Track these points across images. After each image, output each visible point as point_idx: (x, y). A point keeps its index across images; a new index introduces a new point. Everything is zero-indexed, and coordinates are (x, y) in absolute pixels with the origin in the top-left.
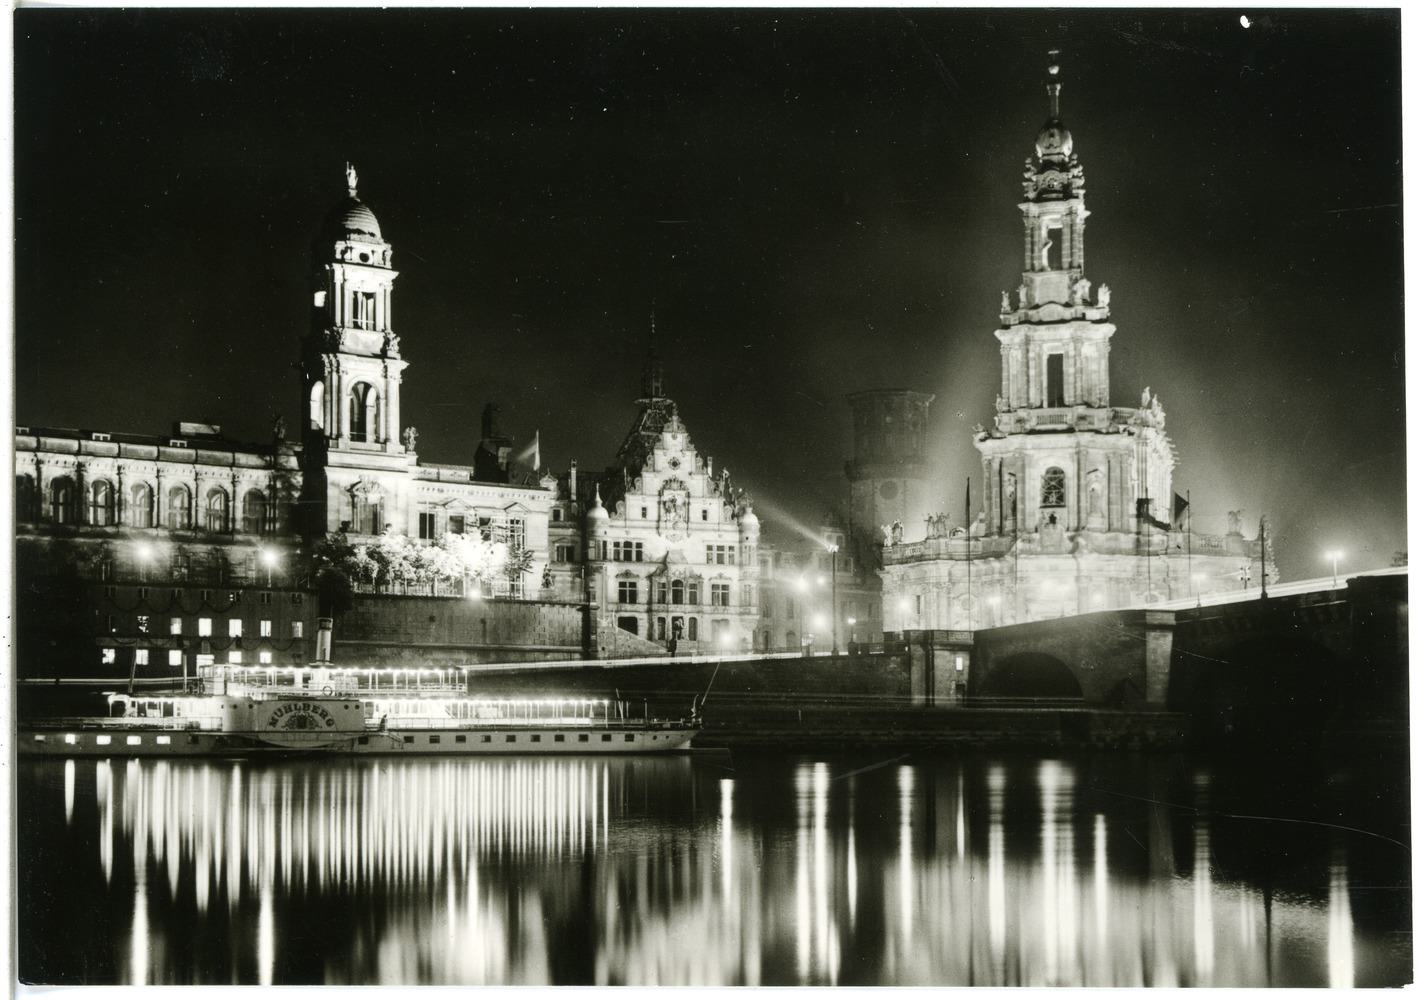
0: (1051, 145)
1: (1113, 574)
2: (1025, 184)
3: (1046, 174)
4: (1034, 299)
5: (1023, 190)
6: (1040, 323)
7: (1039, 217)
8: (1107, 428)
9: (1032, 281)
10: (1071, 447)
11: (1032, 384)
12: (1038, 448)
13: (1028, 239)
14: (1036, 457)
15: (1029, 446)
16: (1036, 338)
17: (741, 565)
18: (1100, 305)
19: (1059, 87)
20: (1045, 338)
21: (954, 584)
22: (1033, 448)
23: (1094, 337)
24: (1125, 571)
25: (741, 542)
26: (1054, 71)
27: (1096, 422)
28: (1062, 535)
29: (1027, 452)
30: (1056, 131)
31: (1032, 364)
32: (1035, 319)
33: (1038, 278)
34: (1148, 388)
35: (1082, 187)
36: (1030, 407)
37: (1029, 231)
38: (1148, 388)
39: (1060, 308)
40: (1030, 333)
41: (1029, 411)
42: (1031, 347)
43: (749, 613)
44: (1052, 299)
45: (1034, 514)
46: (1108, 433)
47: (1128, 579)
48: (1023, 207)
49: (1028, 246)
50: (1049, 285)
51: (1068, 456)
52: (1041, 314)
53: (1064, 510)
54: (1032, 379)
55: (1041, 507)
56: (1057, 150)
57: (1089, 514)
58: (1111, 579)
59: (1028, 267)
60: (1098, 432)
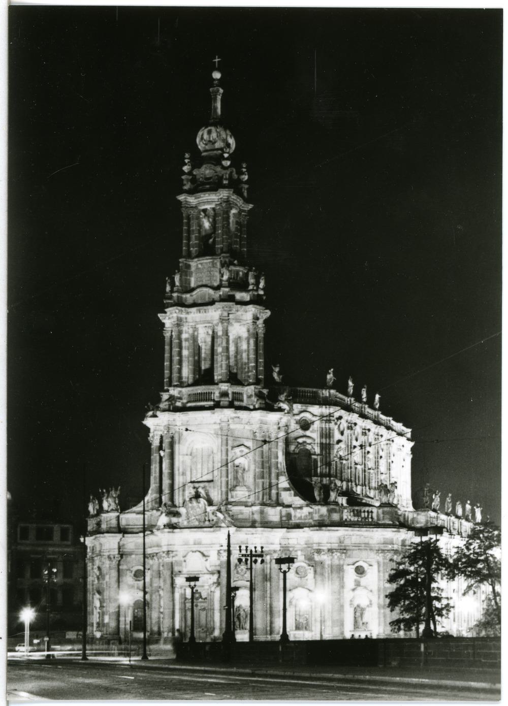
2: (183, 177)
4: (189, 284)
6: (194, 305)
9: (189, 267)
20: (198, 320)
31: (184, 344)
33: (194, 264)
36: (181, 384)
39: (211, 291)
40: (183, 316)
41: (179, 389)
42: (185, 329)
46: (255, 409)
48: (181, 198)
50: (203, 271)
54: (184, 359)
59: (184, 253)
60: (246, 409)
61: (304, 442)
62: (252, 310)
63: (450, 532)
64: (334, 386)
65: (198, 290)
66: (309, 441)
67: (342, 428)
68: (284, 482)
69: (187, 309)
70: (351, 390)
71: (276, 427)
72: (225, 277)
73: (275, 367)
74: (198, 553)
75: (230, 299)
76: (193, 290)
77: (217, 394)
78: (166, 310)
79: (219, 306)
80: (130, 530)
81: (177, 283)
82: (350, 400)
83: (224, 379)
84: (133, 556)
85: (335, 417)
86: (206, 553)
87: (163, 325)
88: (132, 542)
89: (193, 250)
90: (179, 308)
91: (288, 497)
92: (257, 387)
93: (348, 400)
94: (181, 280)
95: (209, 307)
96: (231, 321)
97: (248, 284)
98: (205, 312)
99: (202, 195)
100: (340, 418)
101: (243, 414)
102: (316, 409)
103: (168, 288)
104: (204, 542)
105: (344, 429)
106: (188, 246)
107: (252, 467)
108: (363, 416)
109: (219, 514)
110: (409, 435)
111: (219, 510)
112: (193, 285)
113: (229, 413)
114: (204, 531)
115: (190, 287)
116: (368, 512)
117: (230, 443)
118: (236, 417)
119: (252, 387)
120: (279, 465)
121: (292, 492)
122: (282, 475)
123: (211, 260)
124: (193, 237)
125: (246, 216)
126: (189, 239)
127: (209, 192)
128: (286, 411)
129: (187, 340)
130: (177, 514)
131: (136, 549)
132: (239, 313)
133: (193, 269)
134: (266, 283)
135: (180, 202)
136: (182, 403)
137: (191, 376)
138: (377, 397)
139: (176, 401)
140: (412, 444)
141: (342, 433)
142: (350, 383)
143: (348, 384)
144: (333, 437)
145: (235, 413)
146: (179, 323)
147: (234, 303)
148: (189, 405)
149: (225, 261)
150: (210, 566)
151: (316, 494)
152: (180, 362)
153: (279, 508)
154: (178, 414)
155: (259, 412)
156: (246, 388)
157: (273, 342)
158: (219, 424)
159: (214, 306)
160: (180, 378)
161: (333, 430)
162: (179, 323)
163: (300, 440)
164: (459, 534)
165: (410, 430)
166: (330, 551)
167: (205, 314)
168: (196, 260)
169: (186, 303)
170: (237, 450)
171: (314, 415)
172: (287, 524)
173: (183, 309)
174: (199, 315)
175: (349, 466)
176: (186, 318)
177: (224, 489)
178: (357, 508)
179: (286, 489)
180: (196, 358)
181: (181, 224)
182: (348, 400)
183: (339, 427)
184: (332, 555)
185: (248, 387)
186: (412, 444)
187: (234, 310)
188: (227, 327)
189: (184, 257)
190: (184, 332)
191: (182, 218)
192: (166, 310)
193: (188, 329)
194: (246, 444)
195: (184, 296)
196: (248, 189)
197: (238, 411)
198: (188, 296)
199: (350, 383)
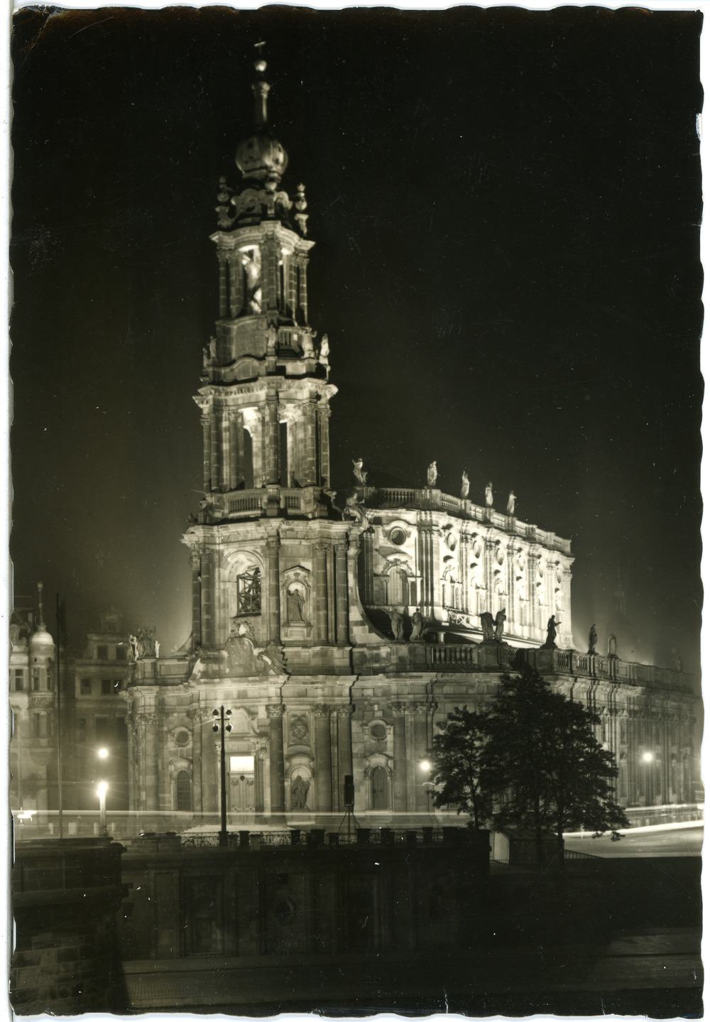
0: (251, 158)
1: (320, 700)
2: (218, 209)
3: (243, 195)
5: (216, 217)
6: (235, 382)
7: (236, 248)
8: (313, 513)
9: (227, 331)
10: (262, 538)
11: (226, 462)
12: (226, 542)
13: (222, 278)
14: (226, 553)
15: (218, 541)
16: (230, 403)
17: (29, 692)
18: (306, 355)
19: (266, 87)
20: (240, 402)
21: (167, 715)
22: (223, 542)
23: (300, 396)
24: (341, 696)
25: (30, 664)
26: (262, 67)
27: (302, 505)
28: (252, 652)
29: (217, 548)
30: (255, 140)
31: (225, 435)
32: (230, 378)
34: (435, 463)
35: (304, 212)
36: (221, 490)
37: (222, 269)
38: (435, 463)
39: (256, 363)
40: (223, 397)
41: (220, 495)
42: (225, 414)
43: (39, 746)
44: (248, 351)
45: (225, 627)
46: (314, 518)
47: (344, 706)
48: (215, 238)
49: (222, 287)
51: (259, 550)
52: (236, 371)
53: (259, 619)
55: (238, 616)
56: (258, 165)
57: (288, 624)
58: (317, 706)
59: (222, 314)
60: (303, 518)
61: (396, 560)
62: (309, 385)
63: (595, 676)
64: (440, 485)
65: (240, 362)
66: (403, 558)
67: (452, 540)
68: (356, 614)
69: (225, 388)
70: (466, 489)
71: (342, 541)
72: (272, 343)
73: (357, 461)
74: (242, 711)
75: (281, 371)
76: (234, 362)
77: (265, 500)
78: (199, 391)
79: (263, 382)
80: (170, 681)
81: (213, 354)
82: (465, 504)
83: (272, 480)
84: (175, 715)
85: (441, 526)
86: (252, 709)
87: (201, 410)
88: (172, 695)
89: (234, 308)
90: (215, 387)
91: (361, 634)
92: (316, 488)
93: (460, 503)
94: (217, 348)
95: (252, 384)
96: (281, 401)
97: (302, 352)
98: (249, 391)
99: (241, 231)
100: (448, 527)
101: (299, 526)
102: (412, 516)
103: (206, 362)
104: (250, 694)
105: (455, 542)
106: (228, 302)
107: (313, 594)
108: (486, 523)
109: (266, 658)
110: (568, 549)
111: (266, 653)
112: (234, 355)
113: (275, 523)
114: (249, 682)
115: (231, 358)
116: (466, 651)
117: (281, 564)
118: (289, 530)
119: (311, 489)
120: (350, 591)
121: (367, 627)
122: (353, 605)
123: (255, 320)
124: (233, 290)
125: (305, 257)
126: (228, 293)
127: (249, 228)
128: (357, 520)
129: (228, 429)
130: (218, 660)
131: (178, 705)
132: (292, 390)
133: (234, 333)
134: (330, 347)
135: (214, 244)
136: (223, 514)
137: (233, 477)
138: (512, 497)
139: (214, 512)
140: (572, 560)
141: (452, 548)
142: (466, 481)
143: (461, 481)
144: (438, 553)
145: (288, 524)
146: (218, 407)
147: (283, 378)
148: (232, 515)
149: (272, 321)
150: (258, 726)
151: (394, 627)
152: (219, 460)
153: (348, 649)
154: (216, 527)
155: (317, 521)
156: (303, 491)
157: (345, 427)
158: (267, 539)
159: (257, 383)
160: (220, 479)
161: (438, 544)
162: (218, 407)
163: (391, 558)
164: (591, 675)
165: (568, 542)
166: (414, 704)
167: (248, 394)
168: (236, 321)
169: (225, 381)
170: (291, 574)
171: (409, 524)
172: (357, 667)
173: (221, 388)
174: (240, 395)
175: (465, 591)
176: (226, 400)
177: (273, 626)
178: (450, 646)
179: (357, 623)
180: (242, 453)
181: (218, 274)
182: (460, 503)
183: (447, 539)
184: (415, 710)
185: (306, 489)
186: (572, 560)
187: (285, 387)
188: (276, 410)
189: (221, 318)
190: (224, 419)
191: (217, 264)
192: (199, 391)
193: (229, 414)
194: (303, 564)
195: (223, 371)
196: (308, 221)
197: (291, 522)
198: (227, 370)
199: (466, 481)
